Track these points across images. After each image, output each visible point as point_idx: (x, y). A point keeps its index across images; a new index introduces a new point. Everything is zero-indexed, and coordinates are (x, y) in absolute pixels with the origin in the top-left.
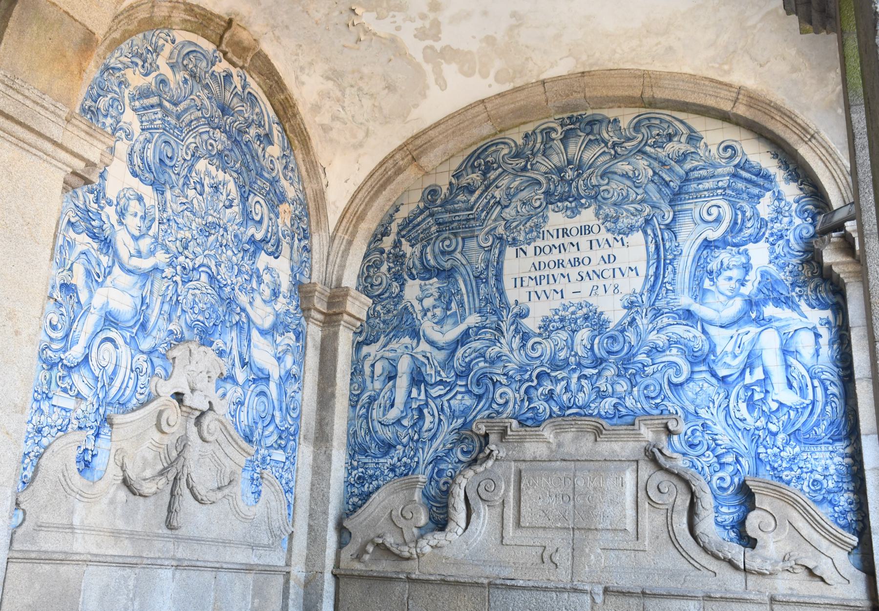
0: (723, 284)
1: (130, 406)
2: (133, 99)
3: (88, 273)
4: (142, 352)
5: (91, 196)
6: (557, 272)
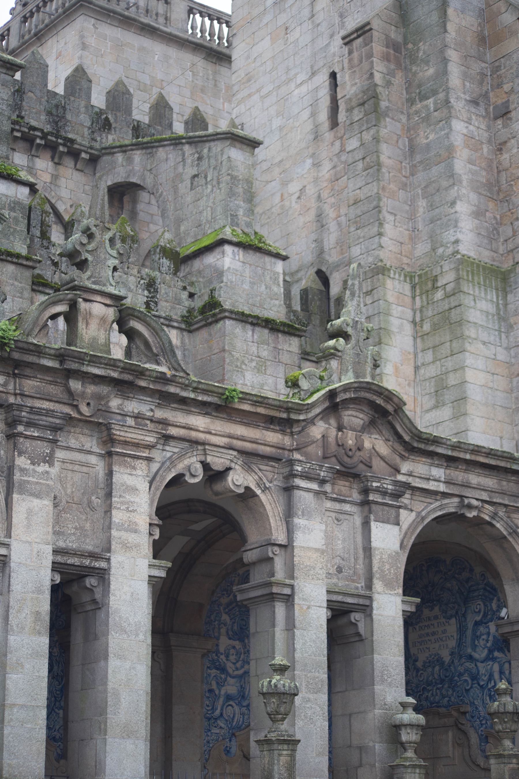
0: (482, 643)
1: (242, 728)
2: (225, 609)
3: (218, 683)
4: (244, 707)
5: (214, 654)
6: (427, 639)
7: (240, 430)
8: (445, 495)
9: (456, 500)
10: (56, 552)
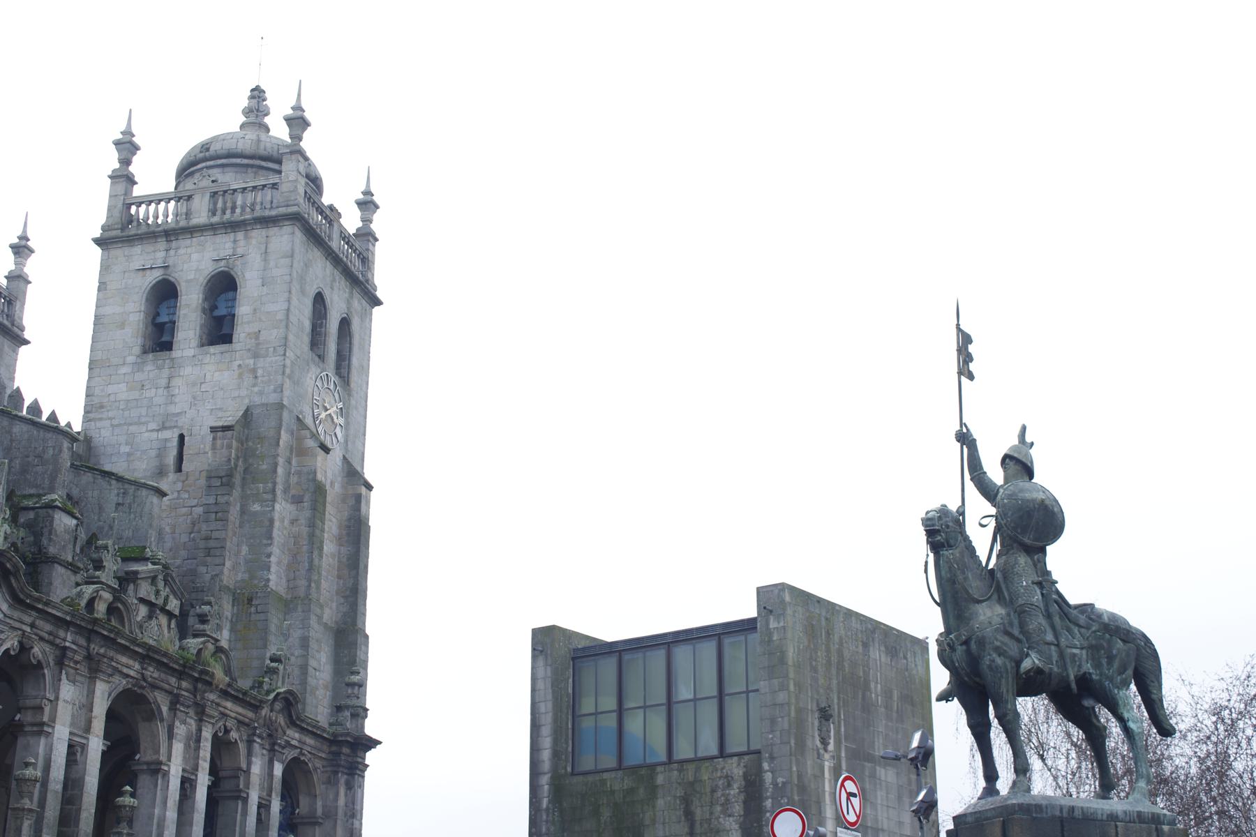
7: (240, 710)
8: (296, 747)
9: (299, 750)
10: (184, 770)
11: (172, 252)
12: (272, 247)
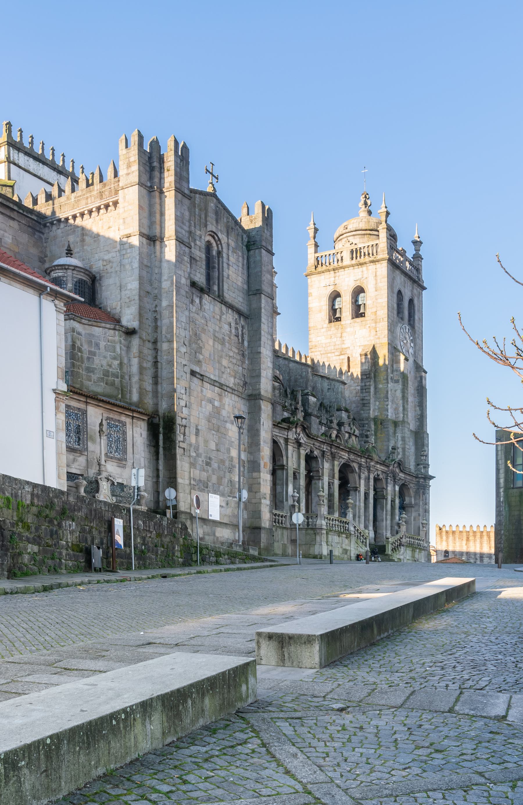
7: (382, 468)
11: (337, 278)
12: (378, 273)
